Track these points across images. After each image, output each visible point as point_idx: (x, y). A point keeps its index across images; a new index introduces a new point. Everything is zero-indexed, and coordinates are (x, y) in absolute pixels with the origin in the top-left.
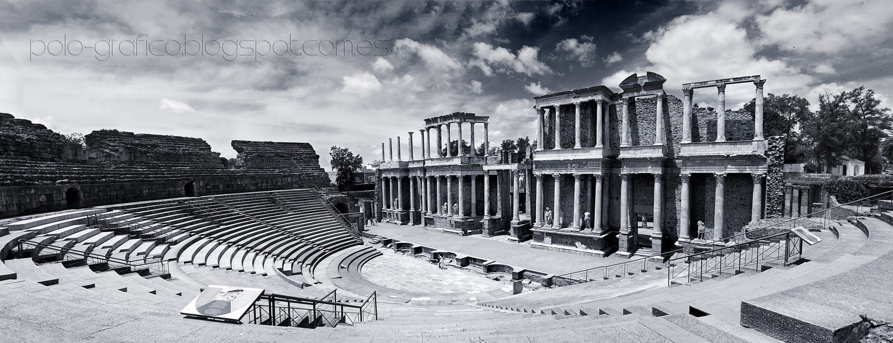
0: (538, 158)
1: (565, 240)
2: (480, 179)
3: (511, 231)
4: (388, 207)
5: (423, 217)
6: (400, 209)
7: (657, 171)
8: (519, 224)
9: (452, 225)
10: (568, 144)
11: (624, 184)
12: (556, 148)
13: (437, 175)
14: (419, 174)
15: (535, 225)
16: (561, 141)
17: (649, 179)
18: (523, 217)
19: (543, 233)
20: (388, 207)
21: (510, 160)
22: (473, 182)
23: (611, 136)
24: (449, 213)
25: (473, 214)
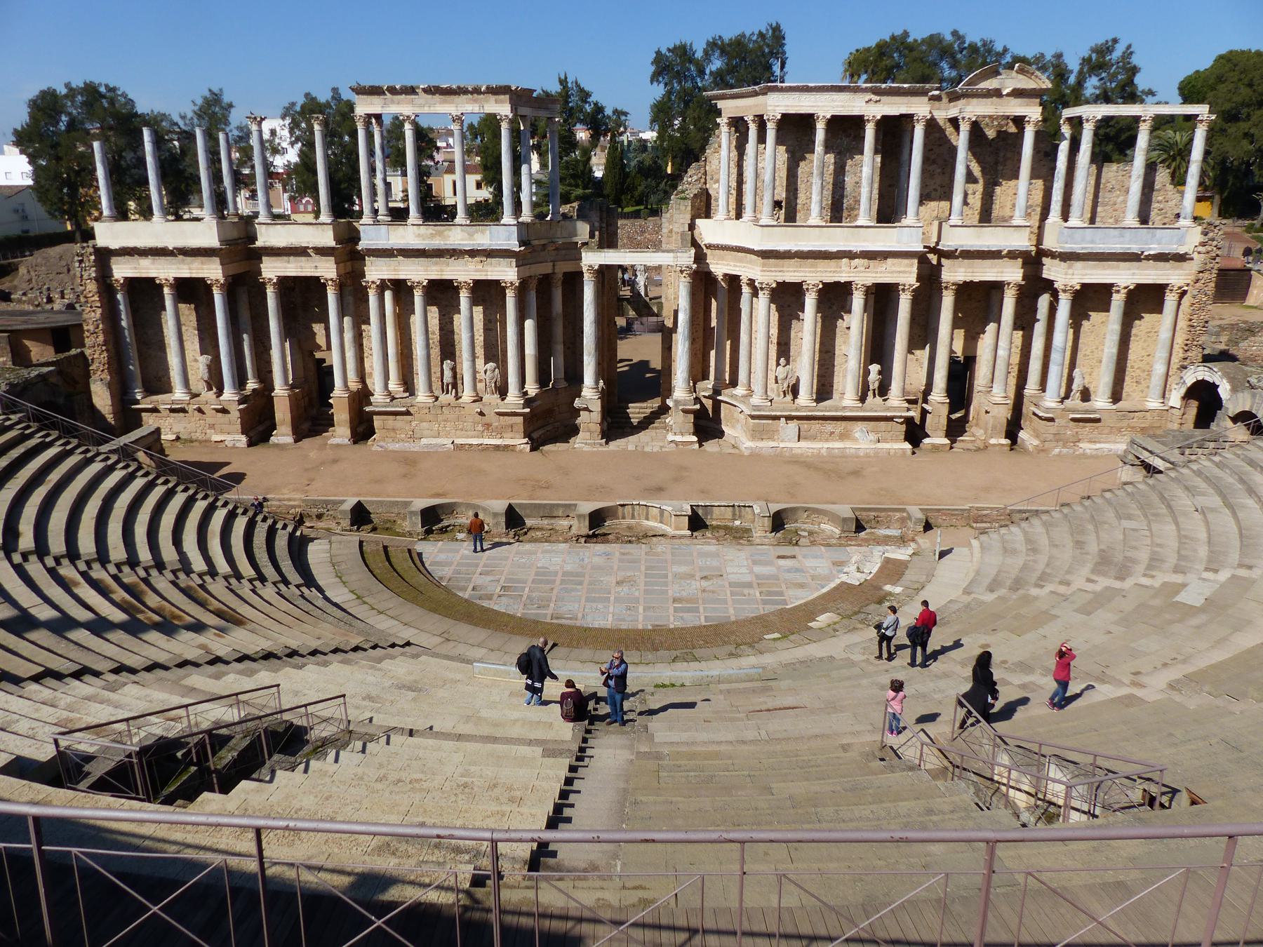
1: (829, 426)
6: (229, 394)
11: (948, 301)
19: (777, 418)
22: (532, 297)
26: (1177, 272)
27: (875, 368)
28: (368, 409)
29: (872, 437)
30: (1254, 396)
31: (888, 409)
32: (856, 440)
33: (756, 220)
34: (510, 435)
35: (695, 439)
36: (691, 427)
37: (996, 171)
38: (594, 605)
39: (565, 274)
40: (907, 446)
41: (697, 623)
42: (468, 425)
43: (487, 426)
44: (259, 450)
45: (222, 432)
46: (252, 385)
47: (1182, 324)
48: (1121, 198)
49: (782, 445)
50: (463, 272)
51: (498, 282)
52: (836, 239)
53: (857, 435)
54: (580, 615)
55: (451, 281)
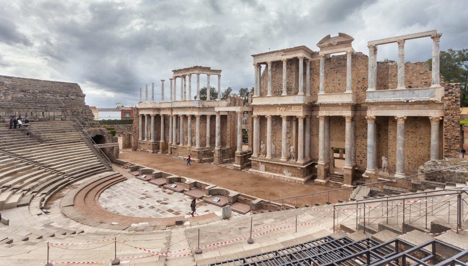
0: (256, 102)
1: (275, 168)
2: (213, 118)
3: (236, 159)
4: (143, 138)
5: (170, 147)
7: (347, 113)
8: (241, 154)
11: (322, 123)
12: (268, 95)
14: (168, 113)
16: (273, 89)
17: (341, 120)
18: (246, 148)
19: (258, 162)
20: (143, 138)
22: (208, 121)
23: (312, 85)
25: (208, 146)
26: (433, 111)
29: (290, 174)
31: (295, 164)
35: (239, 166)
50: (188, 113)
53: (284, 172)
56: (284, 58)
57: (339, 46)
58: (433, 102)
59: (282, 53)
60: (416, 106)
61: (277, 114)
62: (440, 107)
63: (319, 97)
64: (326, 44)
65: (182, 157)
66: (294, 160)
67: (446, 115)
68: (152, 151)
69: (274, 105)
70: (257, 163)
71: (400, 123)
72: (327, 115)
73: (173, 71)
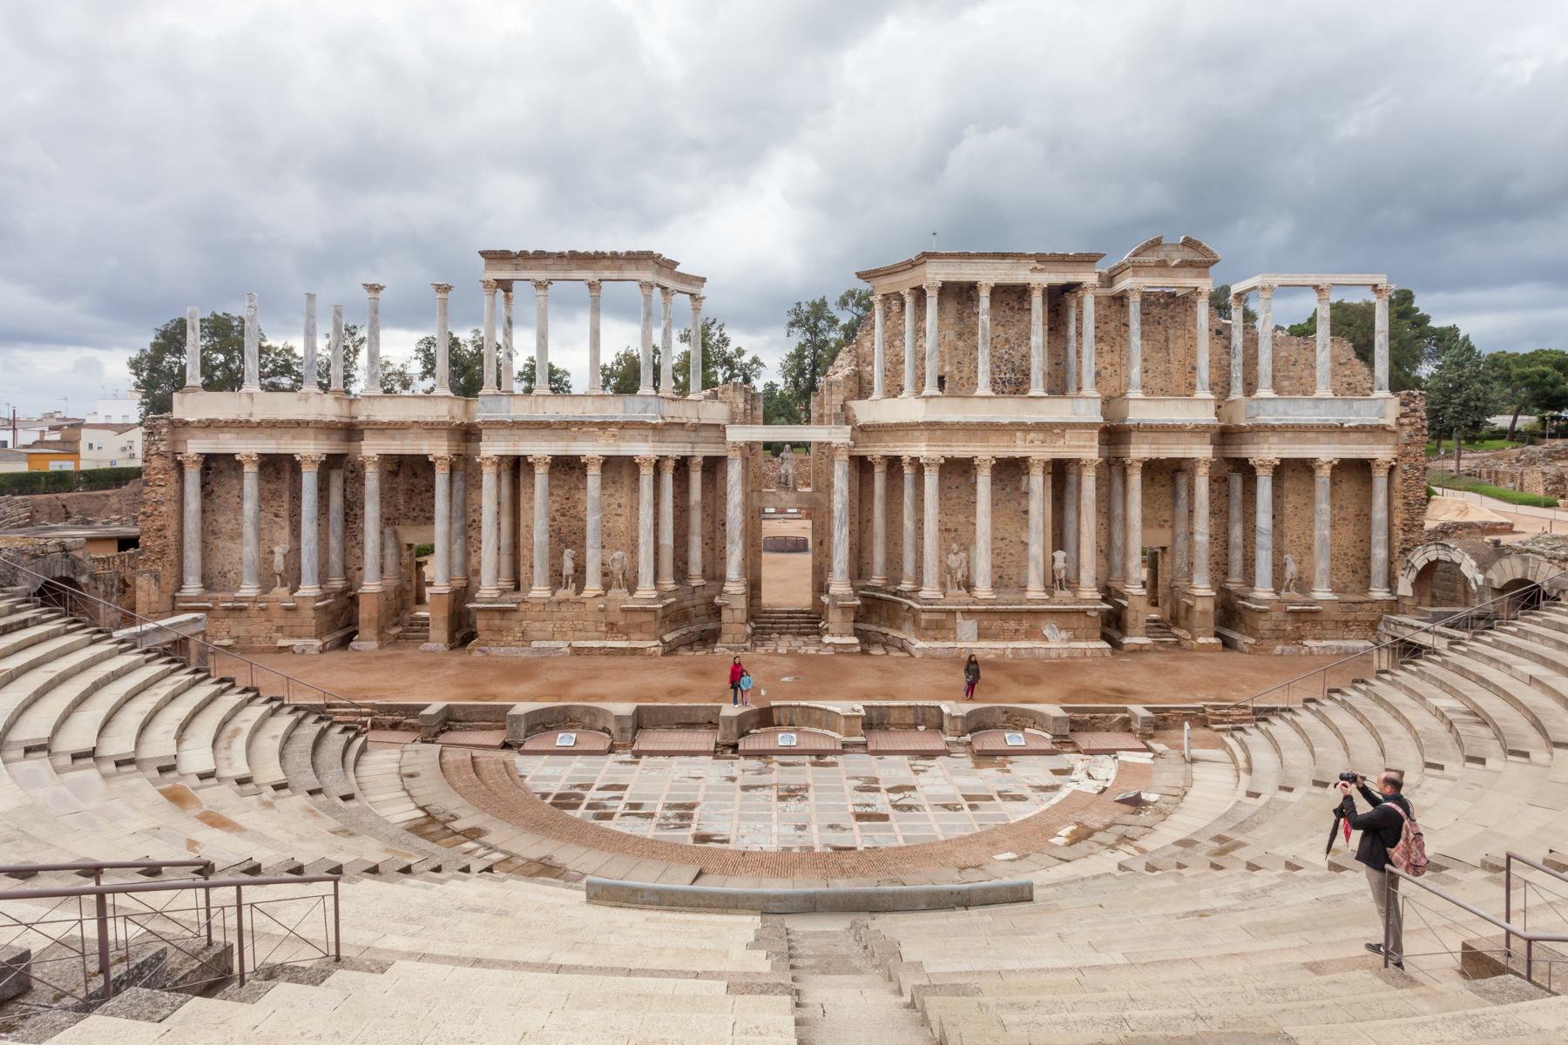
1: (1012, 625)
3: (835, 617)
6: (309, 589)
9: (612, 626)
10: (1013, 383)
11: (1135, 479)
13: (540, 449)
15: (926, 593)
19: (952, 612)
21: (760, 412)
24: (593, 586)
27: (1060, 555)
28: (470, 606)
29: (1064, 635)
30: (1525, 560)
32: (1046, 639)
33: (918, 392)
34: (639, 636)
35: (855, 640)
36: (850, 626)
37: (1167, 348)
38: (751, 824)
39: (705, 458)
40: (1105, 645)
41: (893, 844)
42: (590, 625)
43: (612, 626)
44: (337, 657)
45: (292, 636)
46: (337, 583)
47: (1398, 503)
48: (1307, 372)
49: (959, 645)
50: (590, 449)
51: (631, 458)
52: (1008, 410)
53: (1046, 632)
54: (733, 838)
55: (578, 458)
56: (987, 275)
57: (1181, 272)
58: (1384, 428)
59: (1033, 263)
60: (1353, 436)
61: (1018, 451)
62: (1391, 439)
63: (1132, 404)
64: (1151, 258)
65: (563, 645)
66: (1067, 593)
67: (1405, 455)
68: (318, 643)
69: (1012, 424)
70: (943, 617)
71: (1324, 475)
72: (1154, 456)
73: (483, 254)
